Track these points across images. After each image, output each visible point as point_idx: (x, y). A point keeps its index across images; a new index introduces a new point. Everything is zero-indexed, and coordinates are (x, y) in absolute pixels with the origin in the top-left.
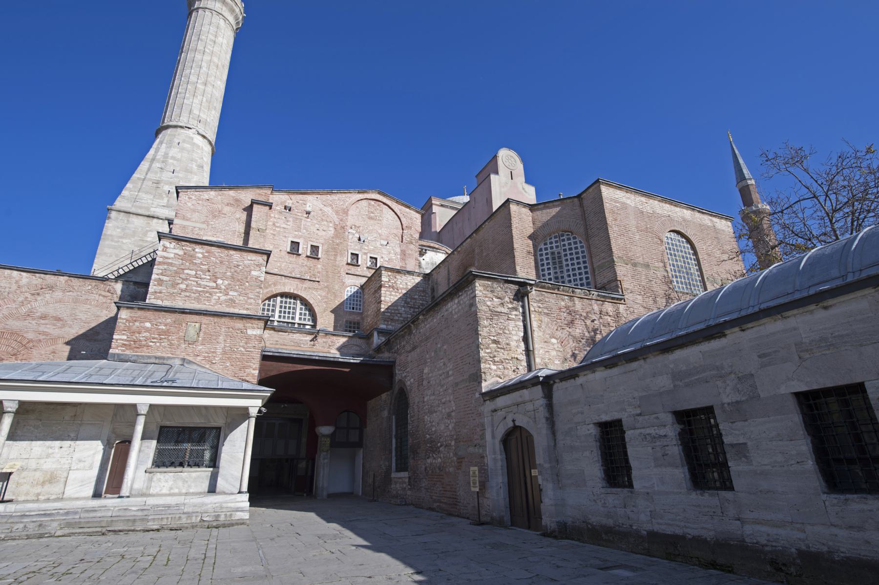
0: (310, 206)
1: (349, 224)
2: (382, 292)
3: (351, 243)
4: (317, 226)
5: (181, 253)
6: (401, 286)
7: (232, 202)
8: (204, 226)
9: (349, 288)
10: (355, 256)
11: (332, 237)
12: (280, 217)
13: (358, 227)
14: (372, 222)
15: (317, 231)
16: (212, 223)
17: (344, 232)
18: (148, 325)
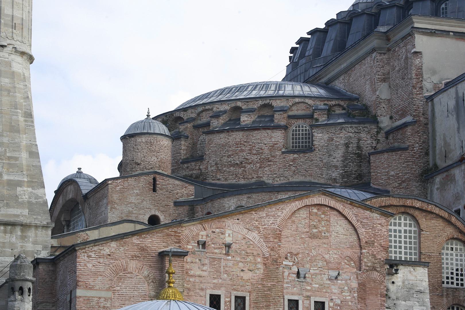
0: (229, 235)
1: (283, 252)
3: (287, 283)
4: (241, 264)
7: (137, 254)
8: (110, 294)
11: (262, 279)
12: (194, 261)
13: (296, 255)
14: (315, 242)
15: (242, 274)
16: (118, 288)
17: (277, 268)
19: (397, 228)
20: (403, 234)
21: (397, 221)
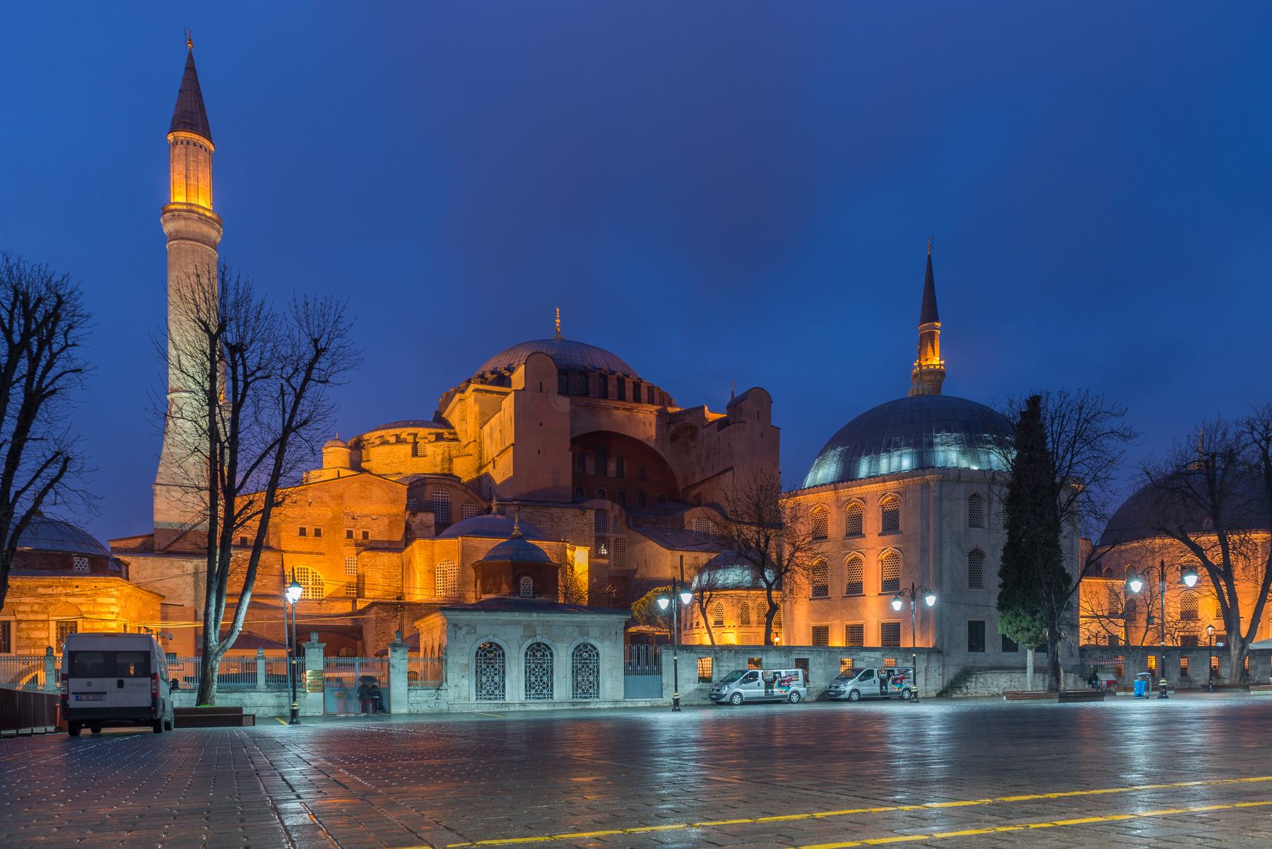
11: (331, 520)
19: (437, 495)
21: (437, 491)
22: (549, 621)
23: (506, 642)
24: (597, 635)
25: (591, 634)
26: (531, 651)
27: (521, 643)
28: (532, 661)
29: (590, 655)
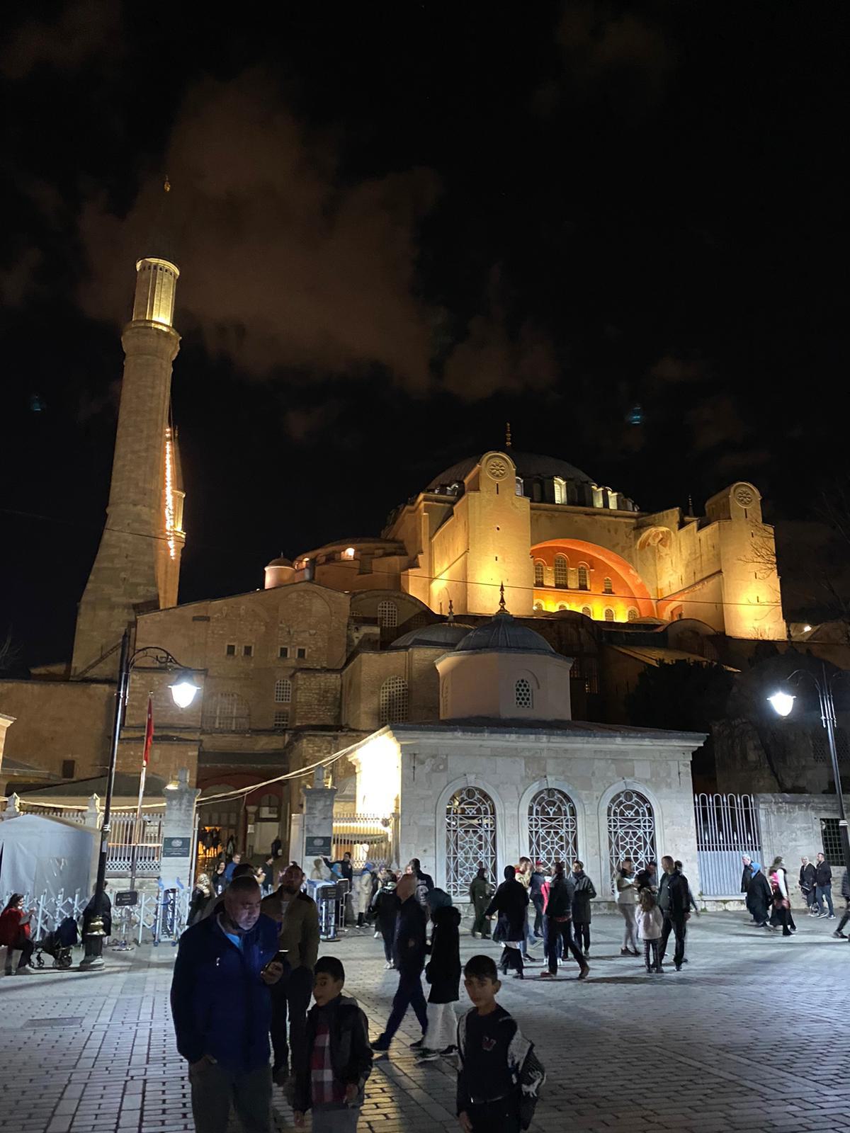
2: (298, 694)
5: (144, 682)
6: (315, 687)
9: (278, 682)
10: (284, 652)
18: (132, 753)
19: (384, 609)
20: (387, 613)
21: (384, 605)
22: (566, 750)
23: (497, 787)
24: (648, 777)
25: (636, 775)
26: (539, 804)
27: (521, 790)
28: (540, 823)
29: (637, 813)
